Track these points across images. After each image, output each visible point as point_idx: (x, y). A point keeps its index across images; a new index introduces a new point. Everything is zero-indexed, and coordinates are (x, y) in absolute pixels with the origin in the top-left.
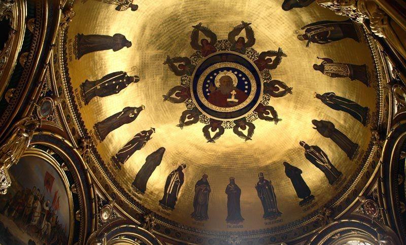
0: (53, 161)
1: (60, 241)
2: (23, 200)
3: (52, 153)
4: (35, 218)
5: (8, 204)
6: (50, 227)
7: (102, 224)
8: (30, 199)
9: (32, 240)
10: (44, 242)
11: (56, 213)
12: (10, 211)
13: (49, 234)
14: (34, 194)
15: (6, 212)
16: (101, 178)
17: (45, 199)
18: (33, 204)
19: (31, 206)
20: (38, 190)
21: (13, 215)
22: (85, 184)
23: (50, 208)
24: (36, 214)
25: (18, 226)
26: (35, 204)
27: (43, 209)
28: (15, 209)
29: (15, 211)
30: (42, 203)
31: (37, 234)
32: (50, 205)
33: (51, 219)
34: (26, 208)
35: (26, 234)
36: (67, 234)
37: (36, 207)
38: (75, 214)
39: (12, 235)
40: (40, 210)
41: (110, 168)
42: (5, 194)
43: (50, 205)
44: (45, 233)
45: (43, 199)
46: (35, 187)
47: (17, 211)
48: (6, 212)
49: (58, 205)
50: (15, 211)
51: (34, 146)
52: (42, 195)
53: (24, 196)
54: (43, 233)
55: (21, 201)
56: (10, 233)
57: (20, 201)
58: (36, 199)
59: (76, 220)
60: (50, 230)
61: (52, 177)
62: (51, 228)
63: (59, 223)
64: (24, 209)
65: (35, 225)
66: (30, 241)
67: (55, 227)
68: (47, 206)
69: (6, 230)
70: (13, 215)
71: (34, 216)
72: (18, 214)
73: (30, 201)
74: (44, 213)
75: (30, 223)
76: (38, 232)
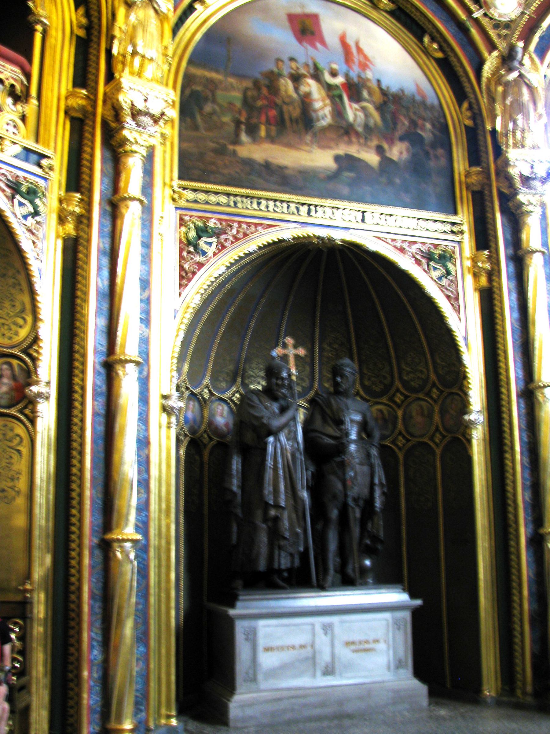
1: (420, 122)
5: (238, 123)
7: (507, 25)
10: (374, 143)
12: (252, 131)
14: (285, 72)
15: (244, 137)
17: (321, 65)
18: (296, 89)
19: (295, 95)
20: (292, 59)
21: (263, 133)
24: (318, 105)
25: (289, 145)
27: (329, 87)
30: (317, 76)
34: (285, 108)
36: (431, 99)
38: (426, 51)
40: (323, 93)
45: (316, 68)
47: (268, 123)
48: (244, 137)
49: (366, 57)
53: (265, 91)
57: (259, 103)
58: (296, 78)
59: (438, 61)
63: (394, 89)
64: (281, 113)
66: (337, 158)
67: (385, 103)
68: (334, 74)
69: (267, 166)
70: (263, 133)
71: (315, 111)
74: (336, 92)
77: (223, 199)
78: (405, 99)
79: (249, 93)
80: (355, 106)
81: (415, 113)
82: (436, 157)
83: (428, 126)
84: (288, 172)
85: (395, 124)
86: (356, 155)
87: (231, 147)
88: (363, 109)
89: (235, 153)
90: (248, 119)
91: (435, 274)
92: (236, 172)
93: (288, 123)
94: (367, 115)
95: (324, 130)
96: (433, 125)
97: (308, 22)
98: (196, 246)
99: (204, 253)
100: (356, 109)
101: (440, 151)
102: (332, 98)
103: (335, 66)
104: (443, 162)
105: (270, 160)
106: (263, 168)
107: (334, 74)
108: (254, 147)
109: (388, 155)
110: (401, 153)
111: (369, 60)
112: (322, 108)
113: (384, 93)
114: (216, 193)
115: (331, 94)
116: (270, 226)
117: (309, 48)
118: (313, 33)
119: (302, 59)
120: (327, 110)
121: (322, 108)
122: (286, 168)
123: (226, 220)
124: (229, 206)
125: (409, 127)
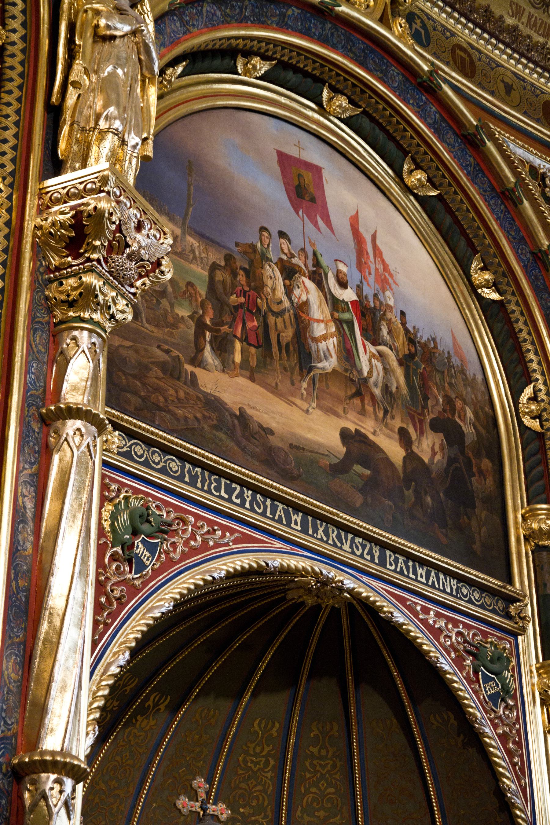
0: (283, 100)
1: (459, 404)
2: (244, 294)
3: (263, 67)
4: (322, 346)
5: (201, 327)
6: (395, 364)
8: (269, 283)
9: (352, 427)
10: (397, 423)
11: (391, 302)
13: (405, 390)
14: (273, 255)
15: (208, 354)
16: (509, 88)
17: (324, 261)
18: (289, 292)
19: (286, 303)
20: (282, 234)
22: (450, 137)
23: (359, 290)
24: (319, 330)
25: (275, 390)
26: (297, 292)
28: (235, 336)
29: (238, 346)
31: (357, 401)
32: (354, 277)
33: (385, 331)
34: (271, 319)
35: (317, 414)
37: (306, 303)
39: (272, 433)
41: (532, 24)
42: (169, 276)
43: (354, 277)
44: (386, 388)
45: (317, 264)
46: (263, 229)
47: (245, 340)
48: (208, 354)
49: (386, 267)
50: (238, 346)
51: (180, 69)
52: (303, 250)
53: (242, 278)
54: (377, 392)
55: (242, 300)
56: (260, 426)
60: (399, 372)
61: (308, 166)
62: (401, 363)
63: (424, 336)
64: (266, 327)
65: (334, 370)
66: (345, 435)
67: (411, 356)
70: (238, 358)
71: (316, 340)
72: (253, 350)
73: (274, 290)
75: (311, 369)
76: (358, 394)
77: (175, 465)
78: (437, 355)
79: (219, 276)
80: (372, 349)
81: (450, 384)
82: (480, 472)
83: (469, 414)
84: (274, 441)
85: (426, 398)
86: (371, 437)
87: (189, 368)
88: (381, 356)
89: (193, 381)
90: (218, 323)
91: (490, 689)
92: (196, 418)
93: (275, 349)
94: (387, 370)
95: (326, 376)
96: (476, 413)
97: (308, 177)
98: (128, 547)
99: (141, 566)
100: (373, 355)
101: (486, 464)
102: (339, 322)
103: (342, 268)
104: (490, 482)
105: (249, 411)
106: (236, 422)
107: (343, 285)
108: (224, 378)
109: (415, 449)
110: (434, 454)
111: (391, 275)
112: (325, 338)
113: (411, 340)
114: (166, 450)
115: (336, 315)
116: (247, 539)
117: (309, 226)
118: (313, 200)
119: (298, 241)
120: (332, 343)
121: (325, 338)
122: (270, 431)
123: (177, 508)
124: (180, 479)
125: (444, 410)
